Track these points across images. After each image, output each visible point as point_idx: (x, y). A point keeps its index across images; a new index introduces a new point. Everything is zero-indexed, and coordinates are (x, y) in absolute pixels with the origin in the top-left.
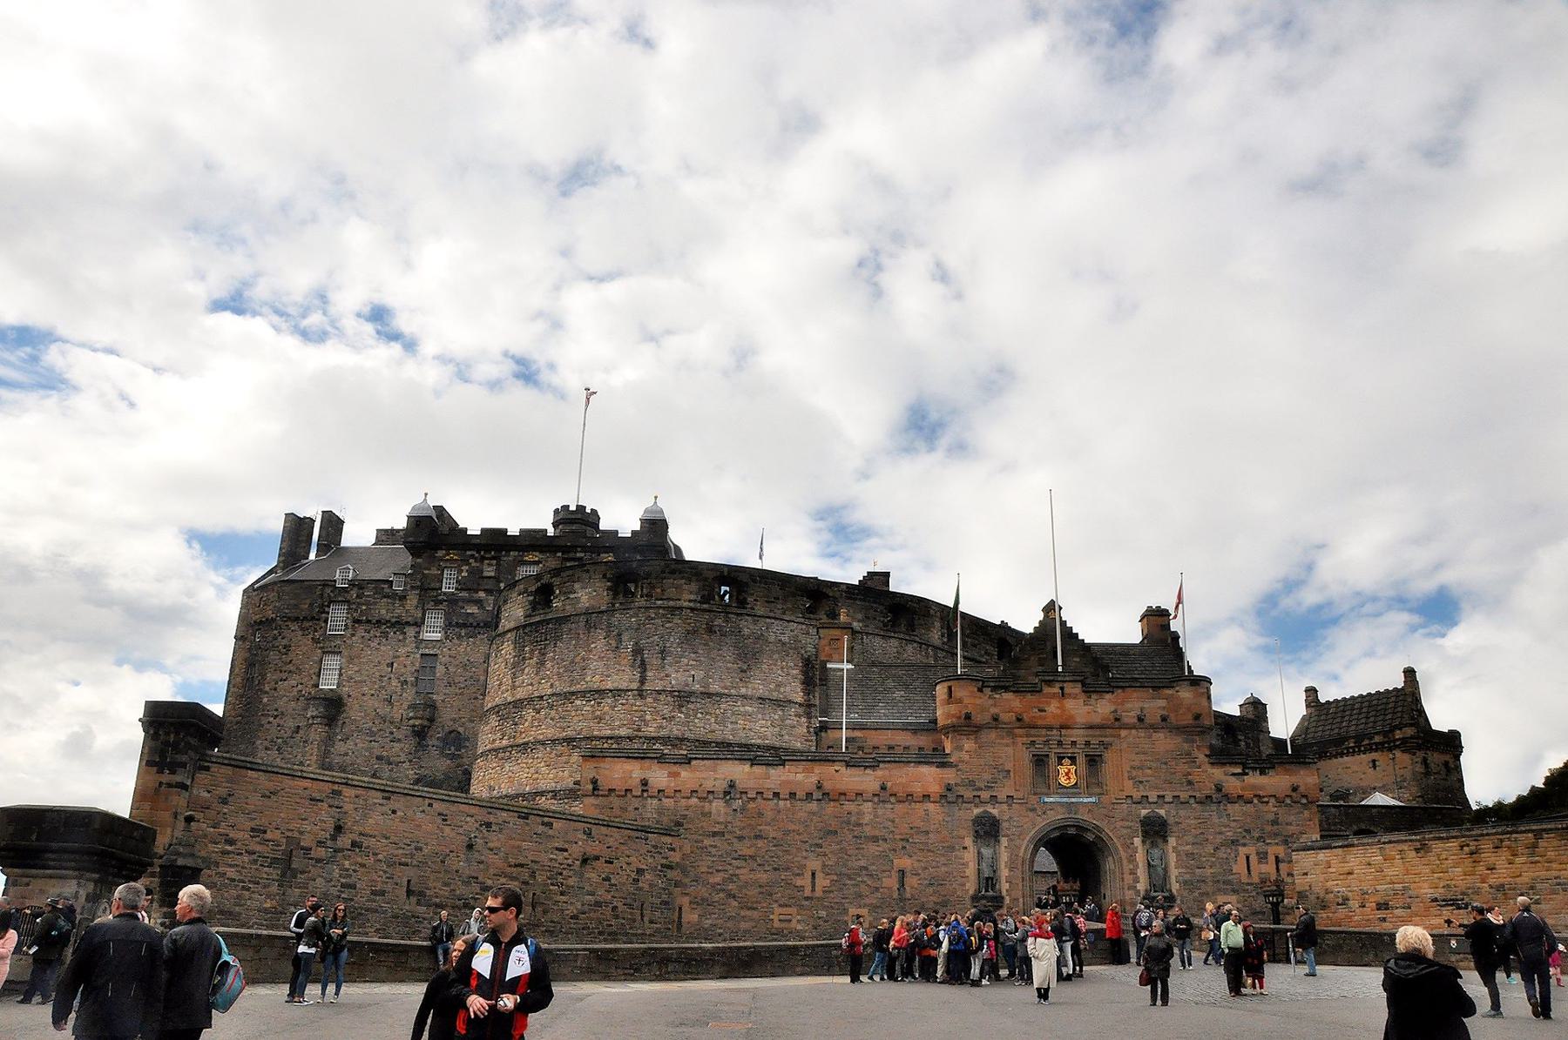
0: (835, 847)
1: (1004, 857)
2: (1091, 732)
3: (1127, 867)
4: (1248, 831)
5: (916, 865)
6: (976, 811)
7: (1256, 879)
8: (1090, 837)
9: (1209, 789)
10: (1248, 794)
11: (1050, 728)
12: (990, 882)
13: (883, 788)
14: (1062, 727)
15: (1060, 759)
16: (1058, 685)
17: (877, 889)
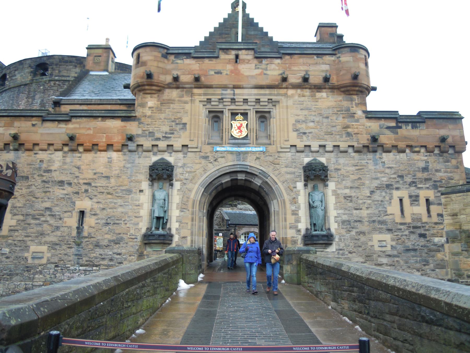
0: (24, 191)
1: (176, 199)
2: (262, 91)
3: (290, 208)
4: (401, 177)
5: (96, 206)
6: (155, 159)
7: (408, 219)
8: (258, 182)
9: (365, 139)
10: (402, 145)
11: (225, 87)
12: (161, 221)
13: (72, 138)
14: (235, 87)
15: (234, 115)
16: (234, 52)
17: (58, 228)
